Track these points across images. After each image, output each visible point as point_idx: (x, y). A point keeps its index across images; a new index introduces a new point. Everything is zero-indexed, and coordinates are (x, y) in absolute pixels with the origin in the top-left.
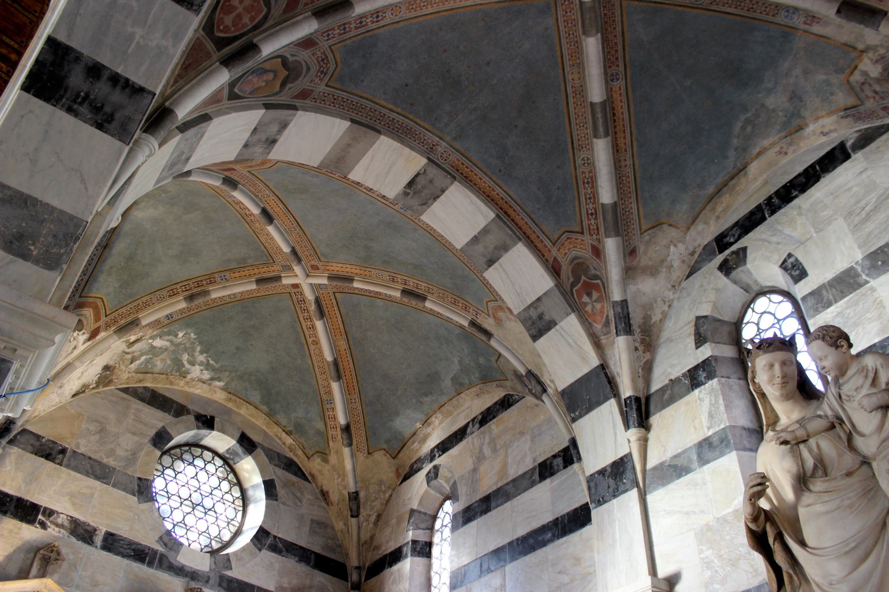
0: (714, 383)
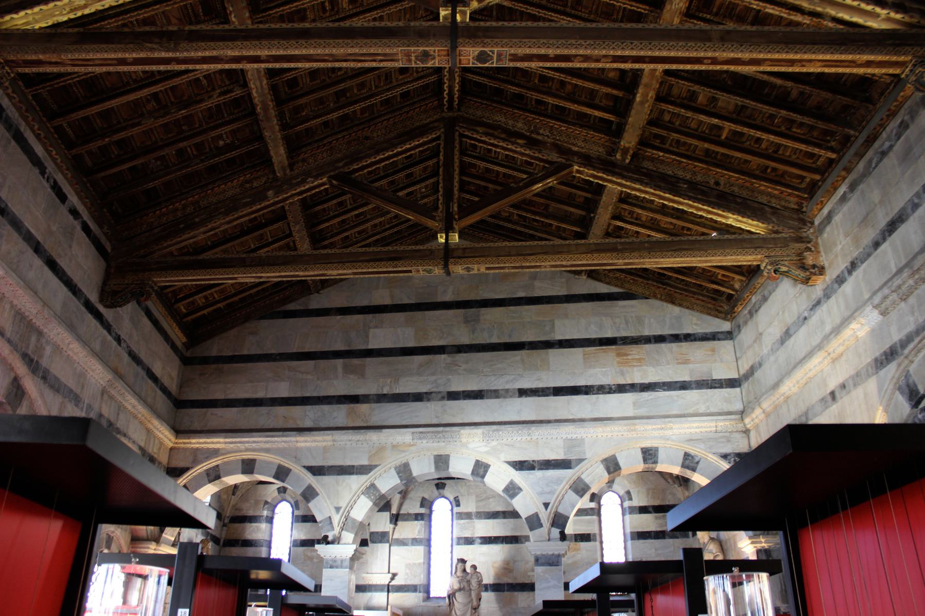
0: (422, 522)
